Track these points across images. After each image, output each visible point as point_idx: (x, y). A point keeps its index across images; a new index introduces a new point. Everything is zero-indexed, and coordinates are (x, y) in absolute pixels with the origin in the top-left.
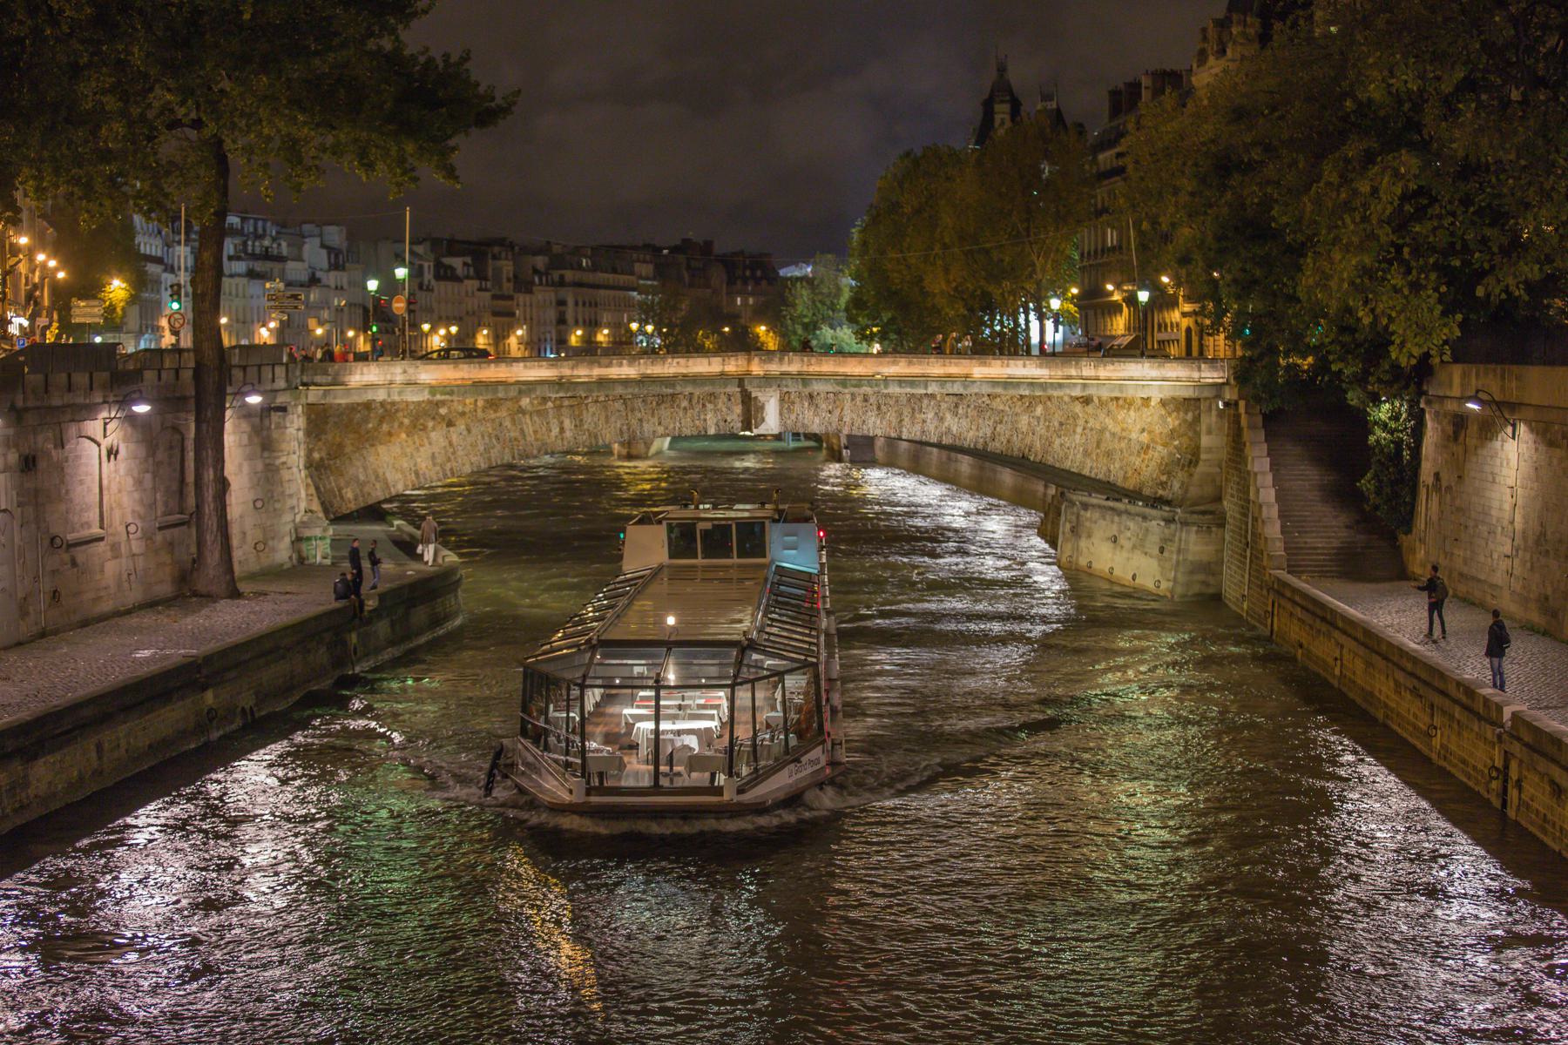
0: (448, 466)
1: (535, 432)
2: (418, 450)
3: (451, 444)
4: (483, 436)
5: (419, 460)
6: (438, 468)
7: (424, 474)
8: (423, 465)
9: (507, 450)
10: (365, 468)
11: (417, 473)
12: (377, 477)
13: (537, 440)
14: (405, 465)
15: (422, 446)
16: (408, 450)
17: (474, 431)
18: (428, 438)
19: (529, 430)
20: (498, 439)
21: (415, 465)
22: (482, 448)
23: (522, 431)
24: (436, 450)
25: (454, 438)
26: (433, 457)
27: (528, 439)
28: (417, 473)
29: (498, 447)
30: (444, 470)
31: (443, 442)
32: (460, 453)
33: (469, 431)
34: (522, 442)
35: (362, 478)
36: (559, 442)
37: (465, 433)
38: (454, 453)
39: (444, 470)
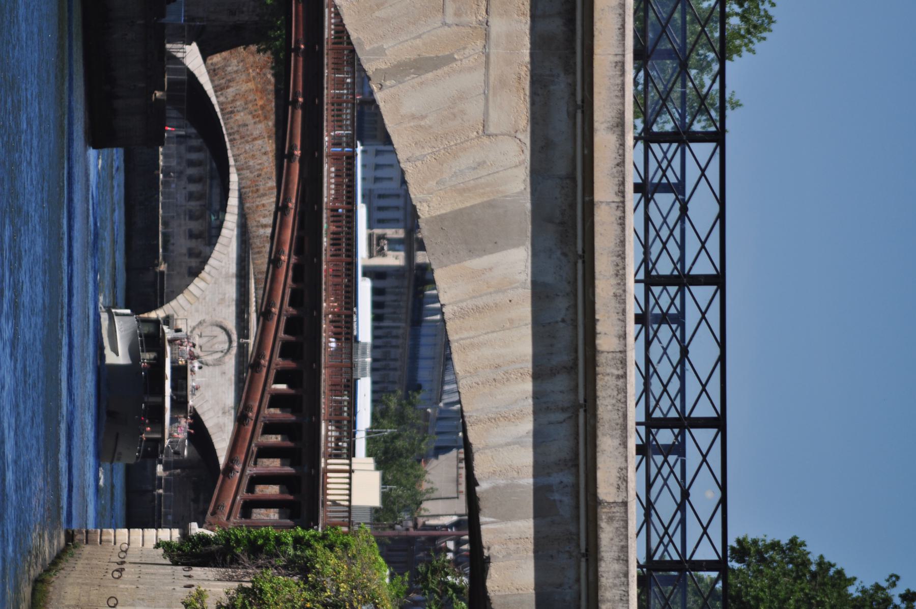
0: (237, 136)
1: (264, 205)
2: (251, 113)
3: (255, 139)
4: (260, 164)
5: (242, 114)
6: (236, 129)
7: (231, 118)
8: (238, 117)
9: (249, 183)
10: (236, 72)
11: (232, 112)
12: (230, 81)
13: (257, 206)
14: (238, 103)
15: (253, 117)
16: (250, 106)
17: (265, 158)
18: (260, 122)
19: (265, 201)
20: (259, 176)
21: (238, 111)
22: (251, 163)
23: (264, 195)
24: (249, 128)
25: (259, 142)
26: (246, 125)
27: (258, 199)
28: (232, 112)
29: (251, 176)
30: (234, 133)
31: (256, 133)
32: (247, 147)
33: (265, 153)
34: (256, 195)
35: (229, 69)
36: (255, 224)
37: (263, 150)
38: (247, 142)
39: (234, 133)
